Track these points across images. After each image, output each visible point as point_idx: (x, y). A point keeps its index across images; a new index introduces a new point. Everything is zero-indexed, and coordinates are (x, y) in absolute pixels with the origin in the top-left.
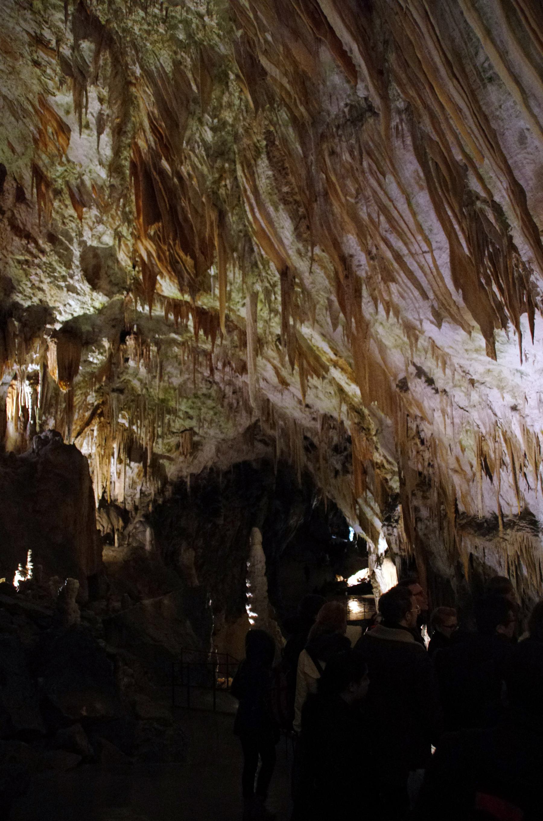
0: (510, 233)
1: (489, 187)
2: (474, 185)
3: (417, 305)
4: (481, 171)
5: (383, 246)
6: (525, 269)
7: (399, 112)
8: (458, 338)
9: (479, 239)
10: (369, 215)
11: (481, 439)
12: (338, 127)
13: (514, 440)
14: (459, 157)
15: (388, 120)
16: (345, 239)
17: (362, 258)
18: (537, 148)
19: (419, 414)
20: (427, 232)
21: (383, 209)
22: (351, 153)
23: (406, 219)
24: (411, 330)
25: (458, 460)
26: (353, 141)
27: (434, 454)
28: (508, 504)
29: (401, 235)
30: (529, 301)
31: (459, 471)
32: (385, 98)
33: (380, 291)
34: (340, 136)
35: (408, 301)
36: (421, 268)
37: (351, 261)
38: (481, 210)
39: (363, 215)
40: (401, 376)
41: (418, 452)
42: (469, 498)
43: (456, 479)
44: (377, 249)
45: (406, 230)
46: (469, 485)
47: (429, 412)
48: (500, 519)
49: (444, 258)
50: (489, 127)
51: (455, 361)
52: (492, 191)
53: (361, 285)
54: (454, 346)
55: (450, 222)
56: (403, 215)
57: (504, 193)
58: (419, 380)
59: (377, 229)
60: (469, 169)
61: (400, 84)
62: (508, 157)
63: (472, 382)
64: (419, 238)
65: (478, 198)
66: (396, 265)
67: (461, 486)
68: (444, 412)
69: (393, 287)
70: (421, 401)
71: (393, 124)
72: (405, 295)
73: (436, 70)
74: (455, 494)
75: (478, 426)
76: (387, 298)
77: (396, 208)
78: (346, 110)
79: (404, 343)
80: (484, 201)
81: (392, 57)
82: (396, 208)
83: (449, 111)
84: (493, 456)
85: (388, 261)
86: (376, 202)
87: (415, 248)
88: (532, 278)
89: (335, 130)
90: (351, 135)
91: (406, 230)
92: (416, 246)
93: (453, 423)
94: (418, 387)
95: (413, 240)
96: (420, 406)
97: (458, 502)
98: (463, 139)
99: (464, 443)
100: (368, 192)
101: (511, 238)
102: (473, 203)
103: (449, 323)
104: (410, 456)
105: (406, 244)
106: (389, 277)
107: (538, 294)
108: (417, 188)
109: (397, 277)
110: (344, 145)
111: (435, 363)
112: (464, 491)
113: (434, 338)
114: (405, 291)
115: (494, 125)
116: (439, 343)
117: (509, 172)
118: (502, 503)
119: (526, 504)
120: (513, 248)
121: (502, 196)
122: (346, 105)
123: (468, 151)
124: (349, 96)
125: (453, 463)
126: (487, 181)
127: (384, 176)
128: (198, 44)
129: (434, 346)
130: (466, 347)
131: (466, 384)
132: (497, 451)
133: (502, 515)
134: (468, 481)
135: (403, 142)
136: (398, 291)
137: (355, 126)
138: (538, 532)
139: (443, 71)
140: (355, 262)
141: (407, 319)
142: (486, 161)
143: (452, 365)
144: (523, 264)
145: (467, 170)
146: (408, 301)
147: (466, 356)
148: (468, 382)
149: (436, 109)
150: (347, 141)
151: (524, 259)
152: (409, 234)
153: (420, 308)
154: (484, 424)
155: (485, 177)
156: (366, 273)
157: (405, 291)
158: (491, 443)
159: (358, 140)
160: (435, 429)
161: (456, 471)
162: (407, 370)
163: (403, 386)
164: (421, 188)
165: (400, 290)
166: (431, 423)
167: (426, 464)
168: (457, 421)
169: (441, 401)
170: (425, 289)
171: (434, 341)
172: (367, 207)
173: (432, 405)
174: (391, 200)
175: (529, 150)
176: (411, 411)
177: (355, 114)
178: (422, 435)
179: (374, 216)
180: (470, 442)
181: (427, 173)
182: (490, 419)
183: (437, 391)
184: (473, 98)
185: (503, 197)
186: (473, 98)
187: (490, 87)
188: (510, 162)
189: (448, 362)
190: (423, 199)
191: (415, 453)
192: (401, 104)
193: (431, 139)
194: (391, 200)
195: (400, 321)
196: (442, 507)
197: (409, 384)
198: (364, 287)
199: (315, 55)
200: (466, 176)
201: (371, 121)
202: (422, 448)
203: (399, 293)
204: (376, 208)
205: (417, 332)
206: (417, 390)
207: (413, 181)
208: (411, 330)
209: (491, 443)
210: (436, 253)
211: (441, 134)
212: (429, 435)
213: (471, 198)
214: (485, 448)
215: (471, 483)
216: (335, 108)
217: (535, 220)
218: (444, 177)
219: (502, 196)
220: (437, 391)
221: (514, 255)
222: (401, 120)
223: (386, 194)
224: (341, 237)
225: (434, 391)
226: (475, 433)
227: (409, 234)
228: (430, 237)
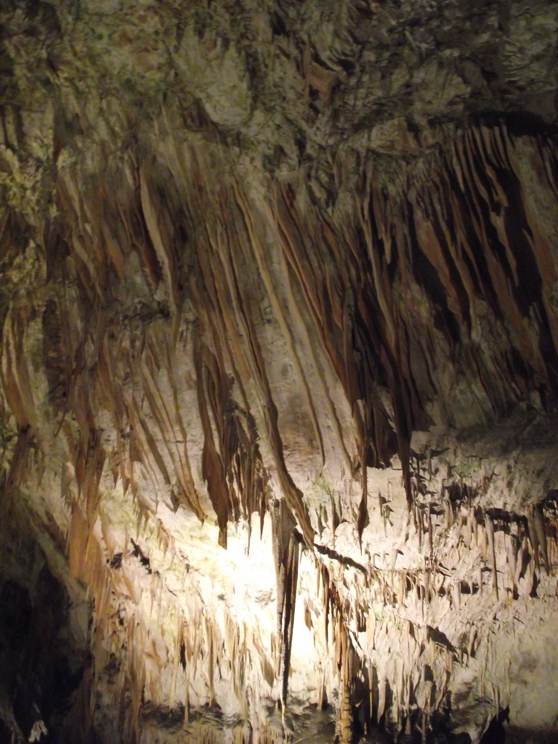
0: (258, 442)
1: (249, 401)
2: (237, 396)
3: (157, 487)
4: (245, 387)
5: (138, 427)
6: (265, 474)
7: (187, 322)
8: (188, 524)
9: (231, 441)
10: (134, 398)
11: (184, 625)
12: (126, 317)
13: (216, 628)
14: (229, 371)
15: (178, 325)
16: (100, 413)
17: (114, 435)
18: (294, 380)
19: (125, 592)
20: (185, 425)
21: (149, 396)
22: (133, 342)
23: (168, 409)
24: (143, 509)
25: (154, 644)
26: (138, 332)
27: (131, 635)
28: (197, 694)
29: (159, 422)
30: (263, 503)
31: (153, 656)
32: (180, 307)
33: (123, 468)
34: (126, 325)
35: (150, 482)
36: (172, 455)
37: (101, 434)
38: (238, 418)
39: (128, 397)
40: (117, 551)
41: (114, 632)
42: (158, 686)
43: (149, 665)
44: (132, 428)
45: (166, 418)
46: (160, 672)
47: (137, 591)
48: (186, 709)
49: (195, 451)
50: (260, 355)
51: (177, 545)
52: (250, 405)
53: (105, 459)
54: (181, 531)
55: (209, 421)
56: (167, 406)
57: (261, 409)
58: (135, 558)
59: (138, 413)
60: (236, 382)
61: (194, 301)
62: (270, 381)
63: (188, 567)
64: (177, 428)
65: (237, 407)
66: (146, 447)
67: (151, 672)
68: (153, 595)
69: (137, 466)
70: (130, 579)
71: (180, 329)
72: (148, 476)
73: (229, 301)
74: (144, 680)
75: (183, 611)
76: (128, 475)
77: (162, 399)
78: (139, 306)
79: (130, 520)
80: (242, 411)
81: (193, 280)
82: (162, 399)
83: (230, 332)
84: (192, 643)
85: (140, 442)
86: (144, 388)
87: (170, 436)
88: (269, 483)
89: (121, 318)
90: (137, 327)
91: (166, 418)
92: (171, 435)
93: (159, 605)
94: (132, 565)
95: (170, 429)
96: (129, 585)
97: (145, 690)
98: (237, 358)
99: (165, 627)
100: (139, 379)
101: (257, 446)
102: (232, 410)
103: (184, 509)
104: (105, 635)
105: (162, 431)
106: (136, 456)
107: (271, 497)
108: (185, 386)
109: (145, 458)
110: (127, 333)
111: (157, 544)
112: (154, 677)
113: (163, 521)
114: (148, 472)
115: (264, 354)
116: (166, 526)
117: (268, 393)
118: (191, 692)
119: (214, 695)
120: (258, 455)
121: (258, 411)
122: (140, 302)
123: (238, 368)
124: (145, 296)
125: (149, 648)
126: (247, 396)
127: (159, 368)
128: (8, 207)
129: (161, 527)
130: (192, 533)
131: (183, 569)
132: (197, 638)
133: (189, 705)
134: (160, 667)
135: (185, 346)
136: (142, 470)
137: (143, 321)
138: (223, 725)
139: (235, 303)
140: (104, 436)
141: (144, 499)
142: (252, 380)
143: (173, 548)
144: (264, 470)
145: (233, 383)
146: (150, 482)
147: (189, 541)
148: (184, 566)
149: (220, 328)
150: (131, 331)
151: (266, 466)
152: (168, 424)
153: (159, 490)
154: (190, 610)
155: (247, 392)
156: (113, 448)
157: (148, 472)
158: (192, 628)
159: (143, 333)
160: (140, 609)
161: (149, 656)
162: (126, 546)
163: (116, 561)
164: (190, 388)
165: (144, 470)
166: (136, 603)
167: (120, 645)
168: (164, 603)
169: (153, 582)
170: (169, 474)
171: (161, 523)
172: (134, 390)
173: (142, 584)
174: (158, 390)
175: (289, 381)
176: (118, 589)
177: (145, 312)
178: (123, 614)
179: (139, 400)
180: (172, 627)
181: (199, 375)
182: (197, 605)
183: (150, 572)
184: (252, 330)
185: (259, 411)
186: (252, 330)
187: (267, 326)
188: (271, 386)
189: (170, 546)
190: (189, 397)
191: (110, 632)
192: (191, 317)
193: (209, 350)
194: (158, 390)
195: (136, 500)
196: (127, 694)
197: (123, 561)
198: (107, 461)
199: (125, 255)
200: (231, 388)
201: (160, 321)
202: (120, 628)
203: (143, 473)
204: (142, 393)
205: (149, 512)
206: (130, 567)
207: (183, 380)
208: (143, 509)
209: (192, 628)
210: (189, 445)
211: (219, 350)
212: (130, 615)
213: (231, 407)
214: (185, 634)
215: (163, 669)
216: (130, 302)
217: (281, 436)
218: (213, 383)
219: (258, 411)
220: (150, 572)
221: (258, 460)
222: (187, 329)
223: (156, 384)
224: (97, 411)
225: (147, 571)
226: (179, 617)
227: (168, 424)
228: (186, 429)
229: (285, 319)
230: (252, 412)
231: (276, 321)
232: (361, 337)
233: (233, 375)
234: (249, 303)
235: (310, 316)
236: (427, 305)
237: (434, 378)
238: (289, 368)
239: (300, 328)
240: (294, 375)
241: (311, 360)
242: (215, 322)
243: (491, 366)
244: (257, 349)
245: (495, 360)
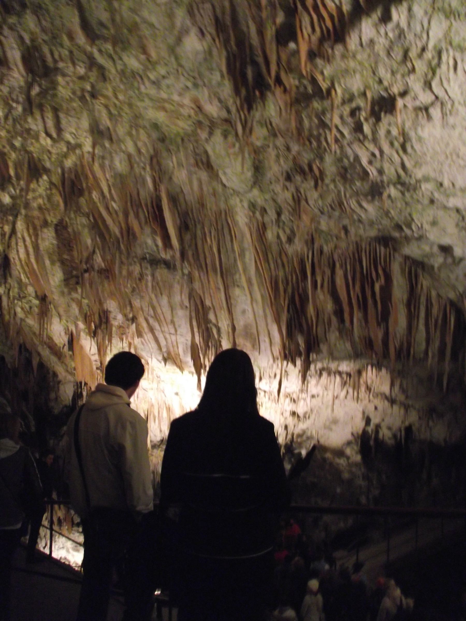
229: (249, 288)
230: (220, 325)
231: (244, 288)
232: (292, 309)
233: (210, 305)
234: (227, 275)
235: (265, 291)
236: (332, 305)
237: (327, 337)
238: (247, 311)
239: (258, 296)
240: (250, 315)
241: (261, 312)
242: (202, 277)
243: (357, 339)
244: (228, 298)
245: (359, 337)
